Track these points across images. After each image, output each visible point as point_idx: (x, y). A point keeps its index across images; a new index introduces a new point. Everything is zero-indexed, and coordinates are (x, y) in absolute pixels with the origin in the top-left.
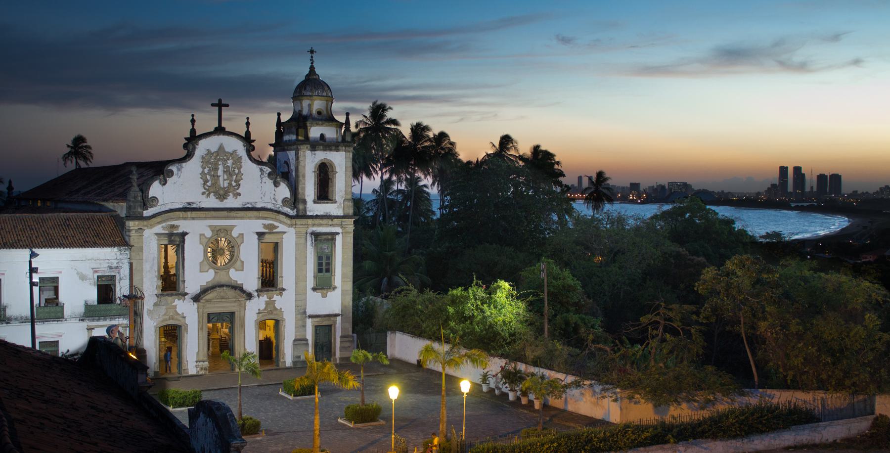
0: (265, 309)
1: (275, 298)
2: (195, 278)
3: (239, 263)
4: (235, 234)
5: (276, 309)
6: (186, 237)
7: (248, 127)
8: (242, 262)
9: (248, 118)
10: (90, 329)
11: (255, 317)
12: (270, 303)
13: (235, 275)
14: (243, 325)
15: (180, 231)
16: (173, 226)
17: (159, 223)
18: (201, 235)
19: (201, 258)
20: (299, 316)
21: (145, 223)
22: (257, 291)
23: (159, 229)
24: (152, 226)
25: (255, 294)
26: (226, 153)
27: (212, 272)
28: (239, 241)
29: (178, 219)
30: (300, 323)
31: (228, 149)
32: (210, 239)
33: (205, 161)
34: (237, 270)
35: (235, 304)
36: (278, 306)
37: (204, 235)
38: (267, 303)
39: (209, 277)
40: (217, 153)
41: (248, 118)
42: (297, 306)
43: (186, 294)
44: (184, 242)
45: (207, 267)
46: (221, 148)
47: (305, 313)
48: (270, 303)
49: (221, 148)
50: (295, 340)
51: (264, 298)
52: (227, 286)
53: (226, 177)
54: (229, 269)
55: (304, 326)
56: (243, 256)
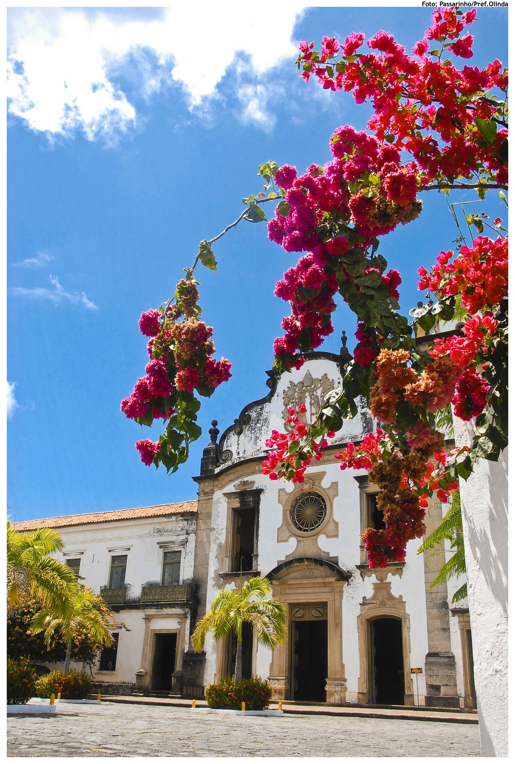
0: (374, 597)
1: (391, 578)
2: (272, 548)
3: (331, 526)
4: (325, 483)
5: (391, 597)
6: (262, 496)
7: (344, 343)
8: (336, 524)
9: (344, 333)
10: (148, 619)
11: (358, 611)
12: (382, 587)
13: (325, 545)
14: (339, 624)
15: (254, 488)
16: (245, 483)
17: (231, 481)
18: (280, 490)
19: (279, 521)
20: (435, 611)
21: (216, 483)
22: (358, 567)
23: (231, 488)
24: (222, 487)
25: (357, 573)
26: (313, 381)
27: (293, 541)
28: (331, 493)
29: (253, 473)
30: (438, 623)
31: (317, 375)
32: (291, 494)
33: (288, 399)
34: (328, 537)
35: (326, 589)
36: (395, 592)
37: (283, 490)
38: (377, 587)
39: (290, 547)
40: (302, 383)
41: (344, 333)
42: (429, 593)
43: (258, 574)
44: (257, 502)
45: (287, 534)
46: (308, 375)
47: (445, 605)
48: (382, 587)
49: (308, 375)
50: (429, 655)
51: (372, 579)
52: (309, 559)
53: (314, 411)
54: (317, 534)
55: (446, 630)
56: (336, 516)
